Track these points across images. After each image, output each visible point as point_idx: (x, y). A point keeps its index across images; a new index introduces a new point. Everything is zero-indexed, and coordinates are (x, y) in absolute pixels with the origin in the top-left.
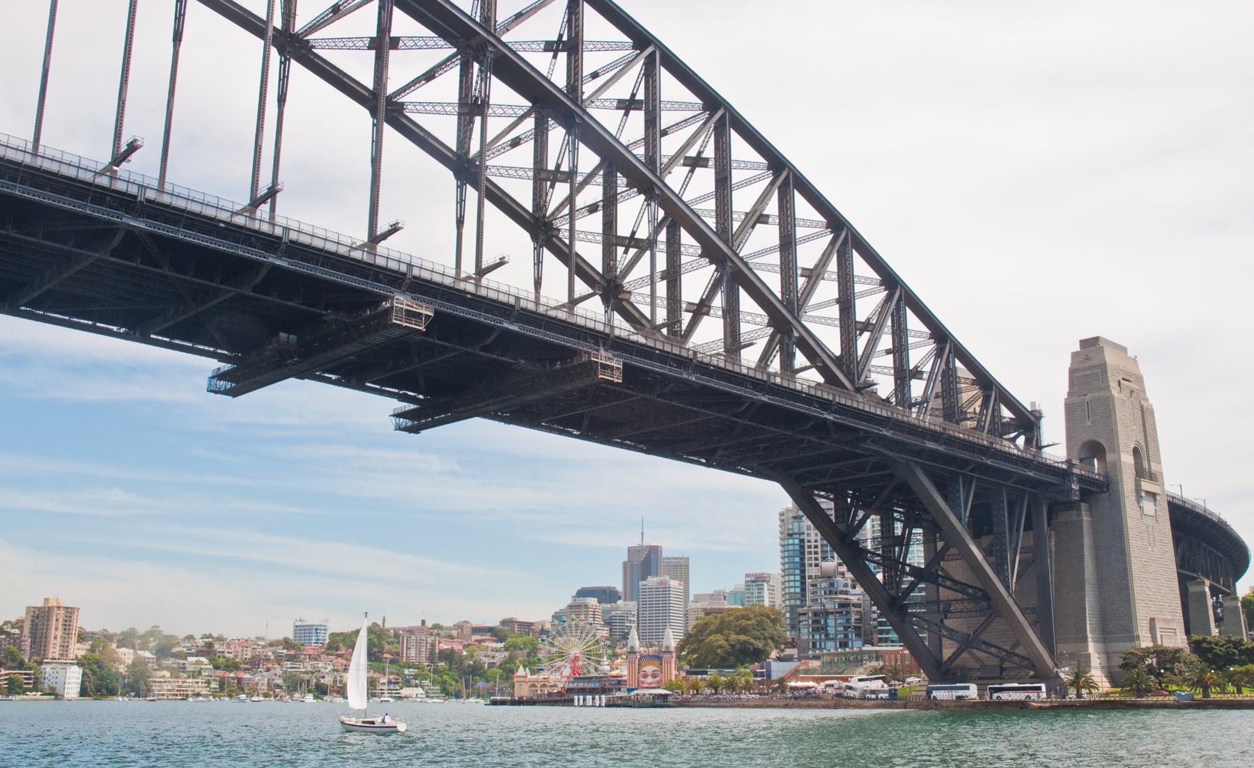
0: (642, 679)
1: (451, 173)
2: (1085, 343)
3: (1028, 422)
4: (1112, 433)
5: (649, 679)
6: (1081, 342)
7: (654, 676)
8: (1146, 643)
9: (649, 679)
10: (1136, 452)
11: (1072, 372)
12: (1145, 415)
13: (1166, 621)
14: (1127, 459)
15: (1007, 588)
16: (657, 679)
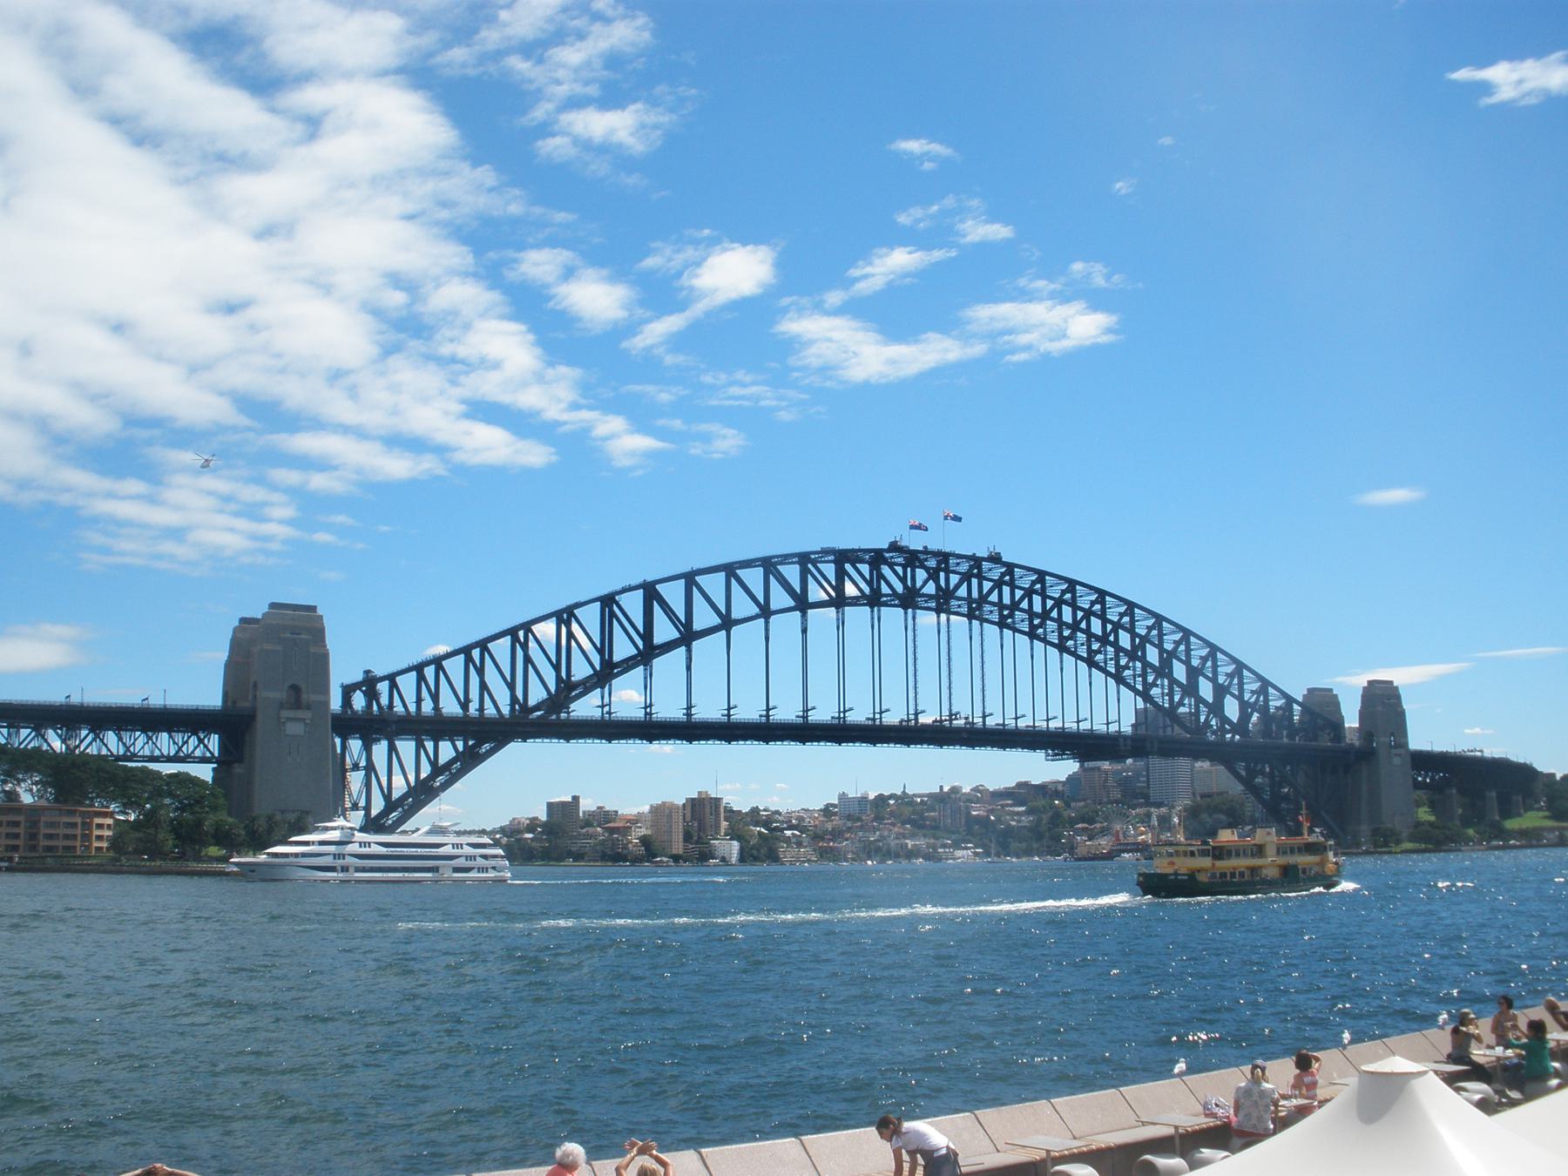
1: (1086, 665)
11: (1363, 696)
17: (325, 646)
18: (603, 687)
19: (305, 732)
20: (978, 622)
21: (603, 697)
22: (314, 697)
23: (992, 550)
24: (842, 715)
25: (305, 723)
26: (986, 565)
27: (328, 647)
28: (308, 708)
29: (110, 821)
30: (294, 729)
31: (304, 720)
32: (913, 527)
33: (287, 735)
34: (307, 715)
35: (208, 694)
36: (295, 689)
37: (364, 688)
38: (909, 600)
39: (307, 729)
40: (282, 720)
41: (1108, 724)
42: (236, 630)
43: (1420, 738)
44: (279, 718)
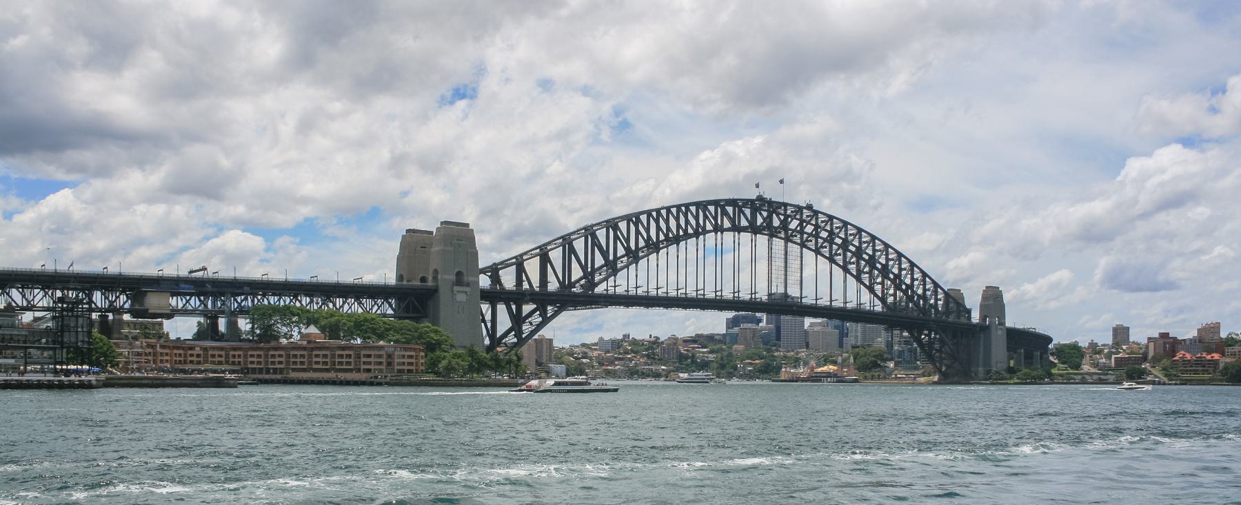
3: (969, 312)
18: (615, 276)
19: (467, 299)
21: (615, 282)
22: (471, 279)
23: (808, 202)
26: (805, 211)
28: (468, 285)
30: (461, 298)
31: (466, 292)
33: (457, 302)
34: (467, 289)
35: (387, 275)
36: (459, 274)
37: (489, 274)
38: (754, 229)
41: (831, 301)
43: (1013, 320)
44: (453, 291)
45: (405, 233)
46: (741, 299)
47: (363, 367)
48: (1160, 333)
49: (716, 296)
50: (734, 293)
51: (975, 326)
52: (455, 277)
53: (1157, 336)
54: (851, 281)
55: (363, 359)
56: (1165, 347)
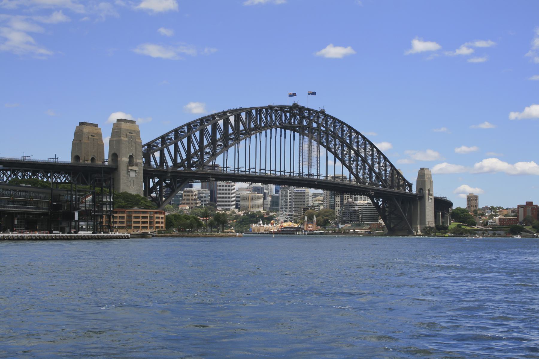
0: (308, 228)
2: (421, 168)
3: (410, 186)
4: (425, 187)
5: (310, 228)
6: (421, 168)
7: (311, 227)
8: (427, 226)
9: (310, 228)
10: (429, 190)
11: (418, 174)
12: (431, 183)
13: (431, 222)
14: (427, 192)
15: (405, 216)
16: (312, 228)
17: (140, 139)
20: (298, 134)
23: (322, 108)
24: (225, 169)
25: (136, 172)
27: (141, 139)
28: (137, 165)
29: (163, 216)
31: (135, 170)
32: (290, 96)
34: (136, 168)
36: (131, 157)
39: (136, 175)
40: (129, 171)
42: (77, 127)
44: (128, 169)
45: (78, 125)
46: (276, 175)
47: (134, 225)
48: (527, 202)
49: (280, 174)
50: (290, 172)
51: (415, 196)
52: (128, 159)
53: (525, 204)
54: (339, 163)
55: (134, 220)
56: (532, 212)
